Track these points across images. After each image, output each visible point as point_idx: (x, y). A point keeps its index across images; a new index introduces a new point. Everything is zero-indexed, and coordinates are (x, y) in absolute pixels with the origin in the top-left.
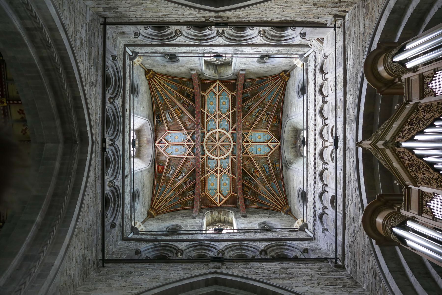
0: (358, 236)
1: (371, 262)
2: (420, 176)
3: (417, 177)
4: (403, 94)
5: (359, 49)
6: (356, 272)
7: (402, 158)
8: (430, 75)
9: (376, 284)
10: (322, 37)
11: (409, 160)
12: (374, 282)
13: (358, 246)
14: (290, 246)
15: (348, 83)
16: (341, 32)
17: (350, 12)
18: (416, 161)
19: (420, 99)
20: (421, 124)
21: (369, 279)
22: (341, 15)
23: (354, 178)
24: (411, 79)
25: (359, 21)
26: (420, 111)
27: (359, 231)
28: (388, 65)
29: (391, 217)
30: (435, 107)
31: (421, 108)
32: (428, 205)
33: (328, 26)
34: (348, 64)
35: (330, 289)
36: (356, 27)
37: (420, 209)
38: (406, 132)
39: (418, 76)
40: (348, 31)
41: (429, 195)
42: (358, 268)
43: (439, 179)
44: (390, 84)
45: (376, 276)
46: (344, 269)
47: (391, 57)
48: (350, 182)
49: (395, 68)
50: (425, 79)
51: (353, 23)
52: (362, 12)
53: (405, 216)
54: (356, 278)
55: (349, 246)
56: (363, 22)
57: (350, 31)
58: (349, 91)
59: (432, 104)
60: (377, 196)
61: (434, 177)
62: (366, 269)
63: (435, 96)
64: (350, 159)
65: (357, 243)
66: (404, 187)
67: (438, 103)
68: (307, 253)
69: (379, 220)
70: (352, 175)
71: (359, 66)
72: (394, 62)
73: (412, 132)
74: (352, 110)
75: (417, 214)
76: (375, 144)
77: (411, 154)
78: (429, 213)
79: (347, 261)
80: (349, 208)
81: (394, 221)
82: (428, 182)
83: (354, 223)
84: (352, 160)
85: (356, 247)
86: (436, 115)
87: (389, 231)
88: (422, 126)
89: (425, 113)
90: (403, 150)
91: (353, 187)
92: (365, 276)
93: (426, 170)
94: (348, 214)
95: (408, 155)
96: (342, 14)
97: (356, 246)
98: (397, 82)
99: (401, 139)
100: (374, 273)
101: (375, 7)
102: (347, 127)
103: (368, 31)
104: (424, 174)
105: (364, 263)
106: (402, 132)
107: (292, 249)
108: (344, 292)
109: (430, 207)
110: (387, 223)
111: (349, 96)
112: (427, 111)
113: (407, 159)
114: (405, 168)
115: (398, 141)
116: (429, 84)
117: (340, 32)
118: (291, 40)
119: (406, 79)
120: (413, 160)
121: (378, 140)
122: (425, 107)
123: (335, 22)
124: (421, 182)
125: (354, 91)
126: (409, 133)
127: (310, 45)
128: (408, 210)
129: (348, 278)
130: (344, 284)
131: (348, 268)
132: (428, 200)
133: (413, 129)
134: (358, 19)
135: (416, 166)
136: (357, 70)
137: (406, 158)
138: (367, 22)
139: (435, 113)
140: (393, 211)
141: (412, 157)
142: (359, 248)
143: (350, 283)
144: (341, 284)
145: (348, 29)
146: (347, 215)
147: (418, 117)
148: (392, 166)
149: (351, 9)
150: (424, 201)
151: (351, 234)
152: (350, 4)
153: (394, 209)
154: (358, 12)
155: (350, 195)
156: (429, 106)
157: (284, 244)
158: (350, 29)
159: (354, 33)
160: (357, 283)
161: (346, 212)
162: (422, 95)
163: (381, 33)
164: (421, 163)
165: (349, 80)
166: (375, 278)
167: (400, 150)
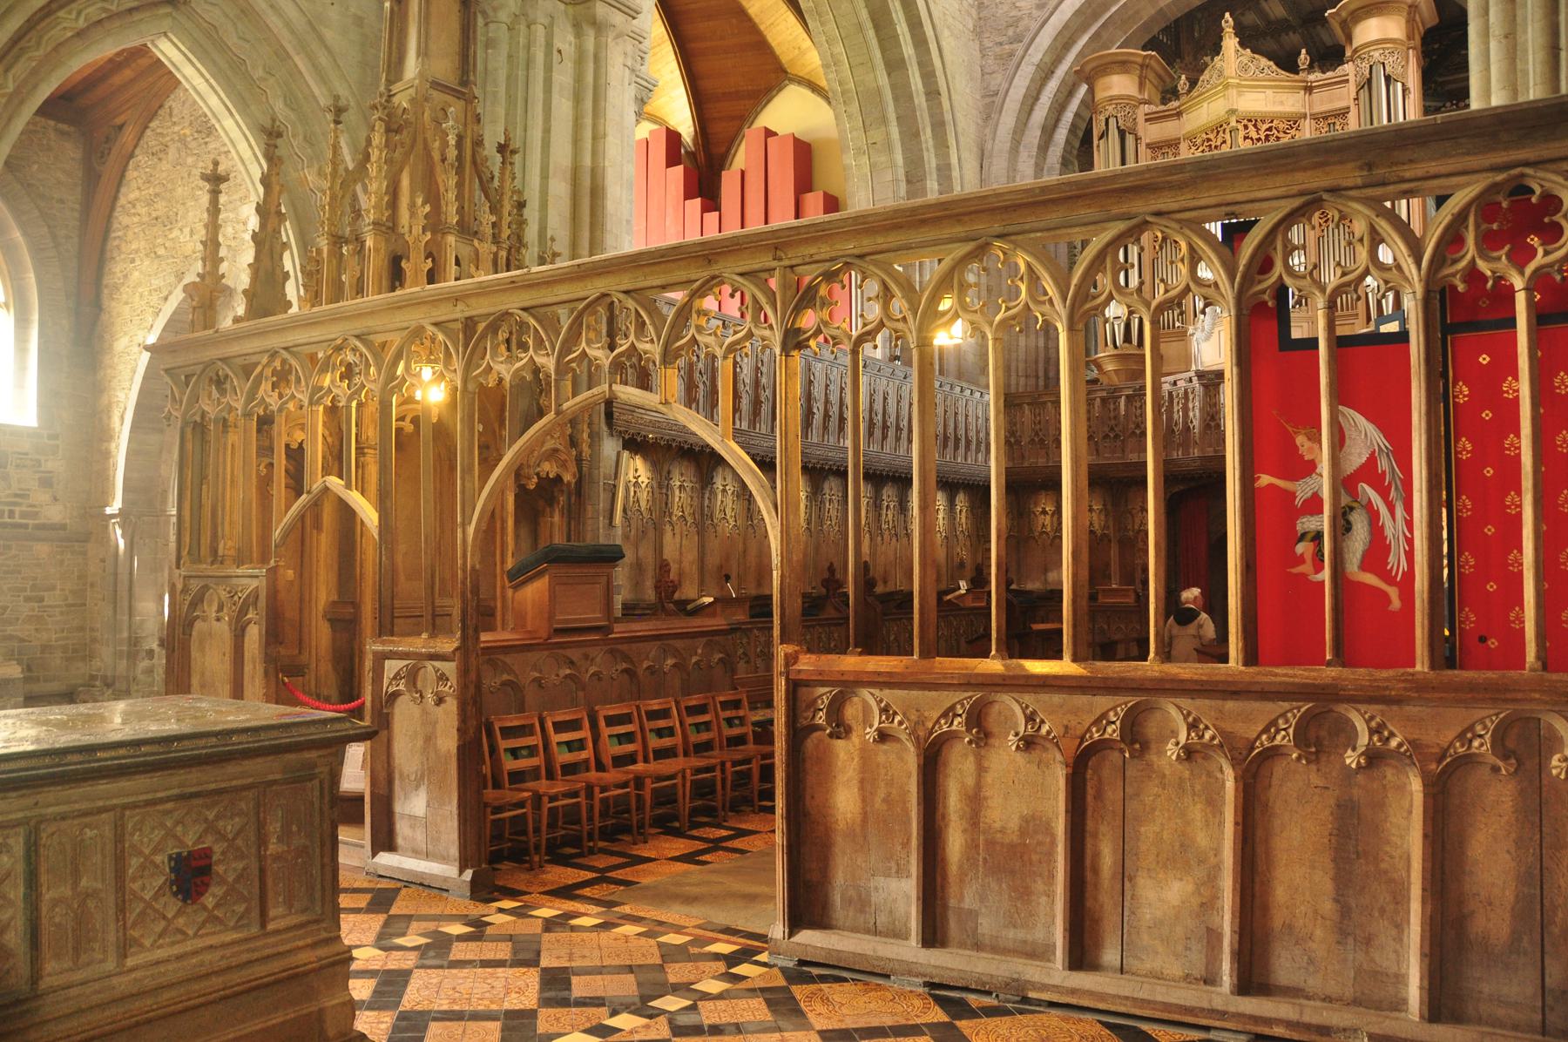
38: (1255, 136)
87: (1107, 114)
90: (1229, 142)
106: (1255, 126)
148: (1204, 100)
162: (1316, 117)
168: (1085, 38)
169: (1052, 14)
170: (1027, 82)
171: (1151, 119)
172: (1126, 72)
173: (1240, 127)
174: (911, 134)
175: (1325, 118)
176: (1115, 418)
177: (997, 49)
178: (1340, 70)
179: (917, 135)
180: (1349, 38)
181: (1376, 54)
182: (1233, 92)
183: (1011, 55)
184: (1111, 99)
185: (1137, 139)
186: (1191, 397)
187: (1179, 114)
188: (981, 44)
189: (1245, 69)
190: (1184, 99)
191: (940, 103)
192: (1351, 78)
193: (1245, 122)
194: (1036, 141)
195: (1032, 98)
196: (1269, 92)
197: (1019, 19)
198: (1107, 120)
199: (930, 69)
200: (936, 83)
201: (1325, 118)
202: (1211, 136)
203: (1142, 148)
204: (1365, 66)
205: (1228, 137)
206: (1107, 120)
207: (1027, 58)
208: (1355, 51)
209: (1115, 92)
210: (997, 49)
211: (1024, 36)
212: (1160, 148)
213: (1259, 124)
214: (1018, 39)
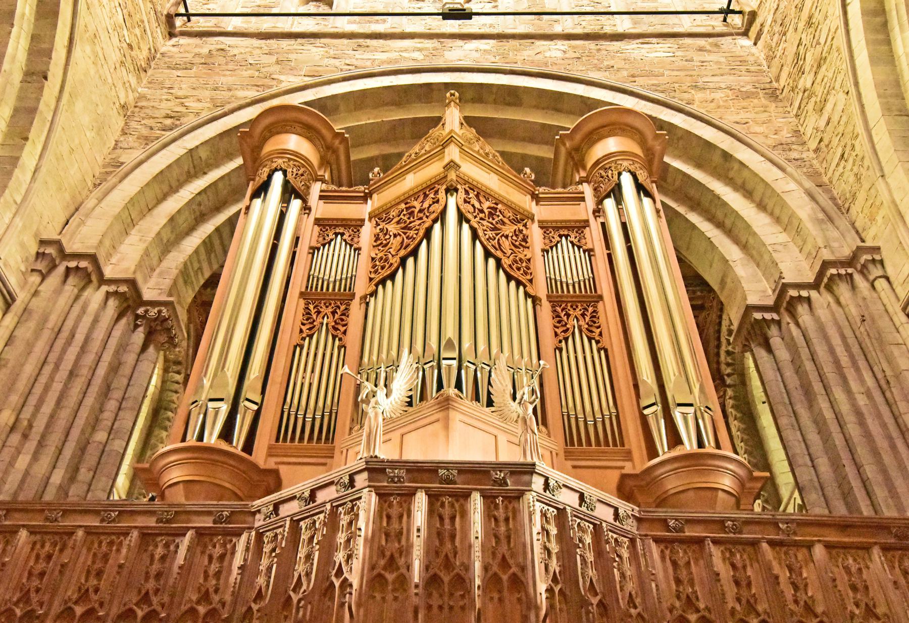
0: (250, 72)
1: (199, 105)
2: (392, 228)
3: (390, 221)
4: (553, 188)
5: (663, 75)
6: (169, 67)
7: (426, 196)
8: (583, 241)
9: (154, 118)
11: (421, 211)
12: (157, 114)
15: (590, 45)
16: (714, 28)
17: (754, 50)
18: (420, 225)
19: (539, 222)
20: (490, 234)
21: (161, 100)
22: (752, 29)
23: (377, 62)
24: (582, 203)
25: (727, 74)
26: (516, 227)
27: (261, 75)
29: (304, 166)
30: (522, 256)
31: (521, 228)
32: (336, 237)
34: (635, 46)
35: (115, 19)
36: (715, 67)
37: (326, 223)
38: (477, 205)
39: (585, 218)
40: (711, 44)
41: (356, 240)
42: (179, 73)
43: (387, 266)
44: (577, 158)
45: (171, 117)
46: (168, 36)
47: (632, 168)
48: (368, 49)
49: (608, 176)
50: (577, 232)
51: (726, 57)
52: (745, 82)
53: (309, 194)
54: (155, 69)
55: (222, 50)
56: (723, 86)
57: (710, 51)
58: (574, 47)
59: (528, 248)
60: (343, 134)
61: (390, 256)
62: (180, 93)
63: (543, 250)
64: (420, 50)
65: (235, 70)
66: (367, 191)
67: (529, 260)
69: (294, 142)
70: (383, 56)
71: (625, 73)
72: (620, 174)
73: (475, 217)
74: (529, 56)
75: (318, 216)
76: (452, 141)
77: (433, 216)
78: (321, 239)
79: (189, 44)
80: (310, 47)
81: (297, 174)
82: (379, 242)
83: (278, 62)
84: (417, 55)
85: (225, 67)
86: (506, 261)
87: (274, 165)
88: (487, 237)
89: (512, 237)
90: (442, 202)
91: (357, 59)
92: (166, 90)
93: (402, 243)
94: (295, 47)
95: (431, 209)
96: (753, 32)
97: (226, 67)
98: (578, 172)
99: (463, 196)
100: (177, 112)
101: (748, 115)
102: (492, 42)
103: (698, 96)
104: (395, 236)
105: (194, 89)
106: (477, 196)
108: (117, 50)
109: (332, 240)
110: (290, 159)
111: (563, 48)
112: (516, 241)
113: (424, 207)
114: (405, 199)
115: (459, 192)
116: (567, 239)
117: (712, 23)
119: (583, 193)
120: (421, 219)
121: (461, 147)
122: (524, 236)
123: (740, 12)
124: (379, 227)
125: (571, 62)
126: (475, 212)
128: (321, 198)
129: (150, 49)
130: (134, 45)
131: (174, 46)
132: (345, 237)
133: (481, 219)
134: (732, 71)
135: (410, 223)
136: (619, 70)
137: (426, 205)
138: (718, 95)
139: (511, 258)
140: (316, 168)
141: (427, 217)
142: (224, 75)
143: (142, 58)
144: (133, 38)
145: (716, 45)
146: (292, 42)
147: (504, 223)
148: (407, 172)
149: (759, 52)
150: (343, 229)
151: (251, 52)
152: (771, 53)
153: (320, 168)
154: (748, 71)
155: (339, 52)
156: (524, 241)
158: (715, 49)
159: (703, 62)
160: (146, 71)
161: (300, 41)
162: (545, 226)
163: (689, 129)
164: (417, 234)
165: (599, 47)
166: (168, 117)
167: (442, 195)
169: (225, 115)
172: (309, 139)
175: (556, 229)
176: (158, 576)
184: (285, 152)
185: (306, 209)
186: (344, 520)
187: (365, 198)
191: (41, 89)
194: (157, 229)
201: (556, 229)
210: (145, 132)
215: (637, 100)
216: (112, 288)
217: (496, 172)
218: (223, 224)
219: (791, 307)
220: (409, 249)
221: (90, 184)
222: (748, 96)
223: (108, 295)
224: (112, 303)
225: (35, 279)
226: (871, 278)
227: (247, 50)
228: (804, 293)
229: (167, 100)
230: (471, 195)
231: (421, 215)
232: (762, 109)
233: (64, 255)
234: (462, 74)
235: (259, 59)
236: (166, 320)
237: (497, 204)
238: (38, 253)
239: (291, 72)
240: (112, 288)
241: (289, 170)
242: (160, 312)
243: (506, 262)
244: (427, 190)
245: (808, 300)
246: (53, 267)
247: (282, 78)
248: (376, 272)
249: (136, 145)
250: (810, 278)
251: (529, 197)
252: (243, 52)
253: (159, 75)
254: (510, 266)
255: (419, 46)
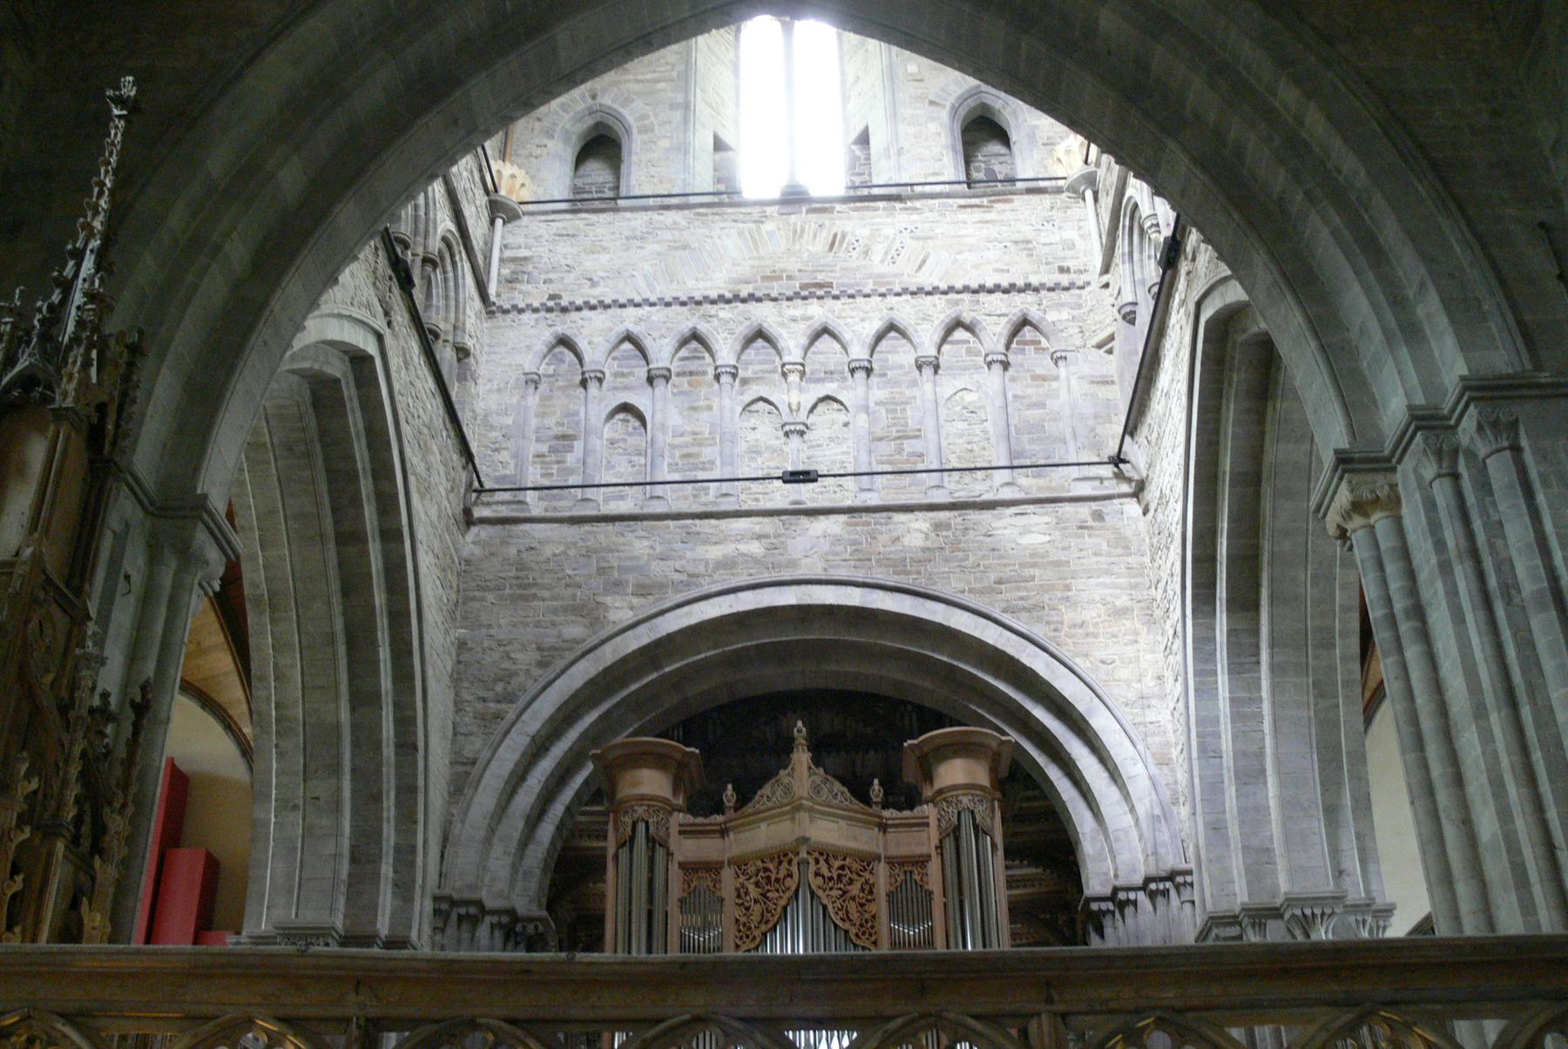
6: (480, 588)
7: (780, 863)
10: (1116, 351)
11: (777, 880)
13: (546, 594)
14: (456, 277)
28: (957, 796)
29: (662, 808)
30: (867, 916)
33: (1127, 438)
38: (827, 874)
42: (490, 597)
47: (971, 806)
63: (888, 895)
64: (759, 537)
67: (874, 917)
68: (459, 360)
75: (681, 859)
77: (789, 894)
83: (601, 571)
87: (636, 816)
93: (762, 915)
106: (827, 861)
107: (452, 294)
110: (649, 806)
118: (1126, 250)
127: (1105, 278)
128: (680, 833)
133: (831, 889)
142: (544, 600)
145: (1099, 516)
148: (763, 820)
157: (457, 258)
162: (891, 862)
166: (498, 679)
168: (592, 717)
170: (516, 756)
171: (685, 832)
173: (812, 861)
174: (368, 797)
175: (902, 864)
177: (480, 706)
178: (917, 811)
179: (377, 798)
180: (929, 777)
181: (965, 800)
182: (804, 816)
183: (498, 717)
184: (642, 798)
187: (723, 832)
188: (457, 694)
189: (817, 789)
190: (731, 814)
192: (933, 822)
193: (816, 855)
195: (519, 777)
196: (842, 823)
197: (513, 674)
198: (634, 824)
199: (409, 713)
200: (415, 734)
201: (902, 864)
202: (771, 866)
203: (674, 868)
204: (953, 811)
205: (795, 869)
206: (634, 824)
207: (518, 726)
208: (940, 792)
209: (645, 790)
211: (517, 697)
212: (696, 870)
213: (831, 860)
214: (509, 698)
215: (1001, 629)
216: (495, 919)
217: (843, 817)
218: (572, 801)
219: (1122, 905)
220: (770, 925)
221: (446, 795)
222: (1122, 613)
223: (493, 926)
224: (498, 934)
225: (438, 938)
226: (1183, 899)
227: (562, 548)
228: (1132, 896)
229: (490, 649)
230: (822, 862)
231: (777, 886)
232: (1132, 638)
233: (454, 903)
234: (810, 587)
235: (576, 566)
236: (541, 934)
237: (844, 859)
238: (435, 911)
239: (616, 589)
240: (495, 919)
241: (650, 821)
242: (536, 927)
243: (853, 930)
244: (782, 855)
245: (1135, 903)
246: (448, 916)
247: (608, 600)
248: (741, 938)
249: (474, 729)
250: (1138, 880)
251: (876, 829)
252: (557, 552)
253: (471, 604)
254: (857, 935)
255: (757, 528)
